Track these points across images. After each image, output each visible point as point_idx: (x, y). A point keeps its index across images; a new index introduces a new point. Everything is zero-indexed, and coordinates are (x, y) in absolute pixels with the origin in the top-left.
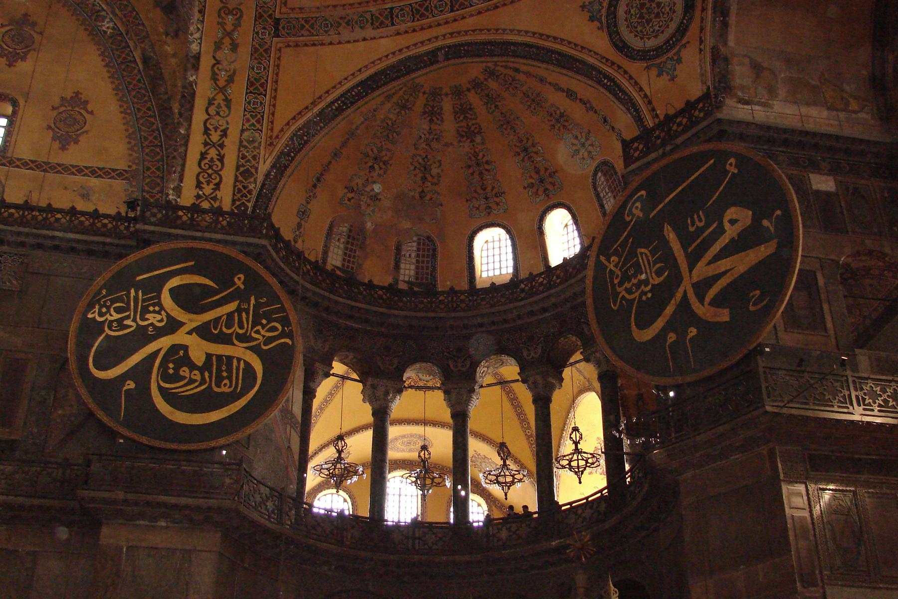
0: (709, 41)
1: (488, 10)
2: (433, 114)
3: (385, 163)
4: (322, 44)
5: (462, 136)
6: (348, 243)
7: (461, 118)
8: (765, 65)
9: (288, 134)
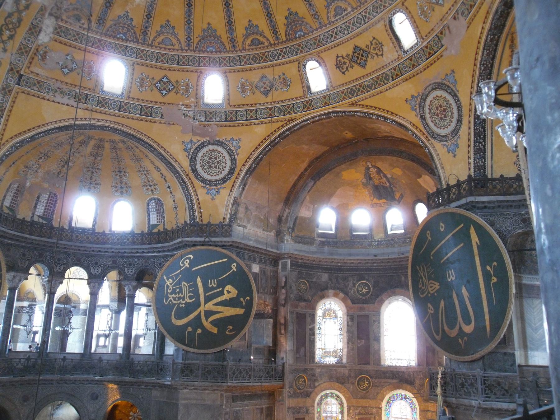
0: (235, 193)
1: (137, 119)
2: (83, 143)
3: (48, 157)
4: (43, 98)
5: (92, 155)
6: (15, 193)
7: (96, 149)
8: (249, 208)
9: (10, 144)
